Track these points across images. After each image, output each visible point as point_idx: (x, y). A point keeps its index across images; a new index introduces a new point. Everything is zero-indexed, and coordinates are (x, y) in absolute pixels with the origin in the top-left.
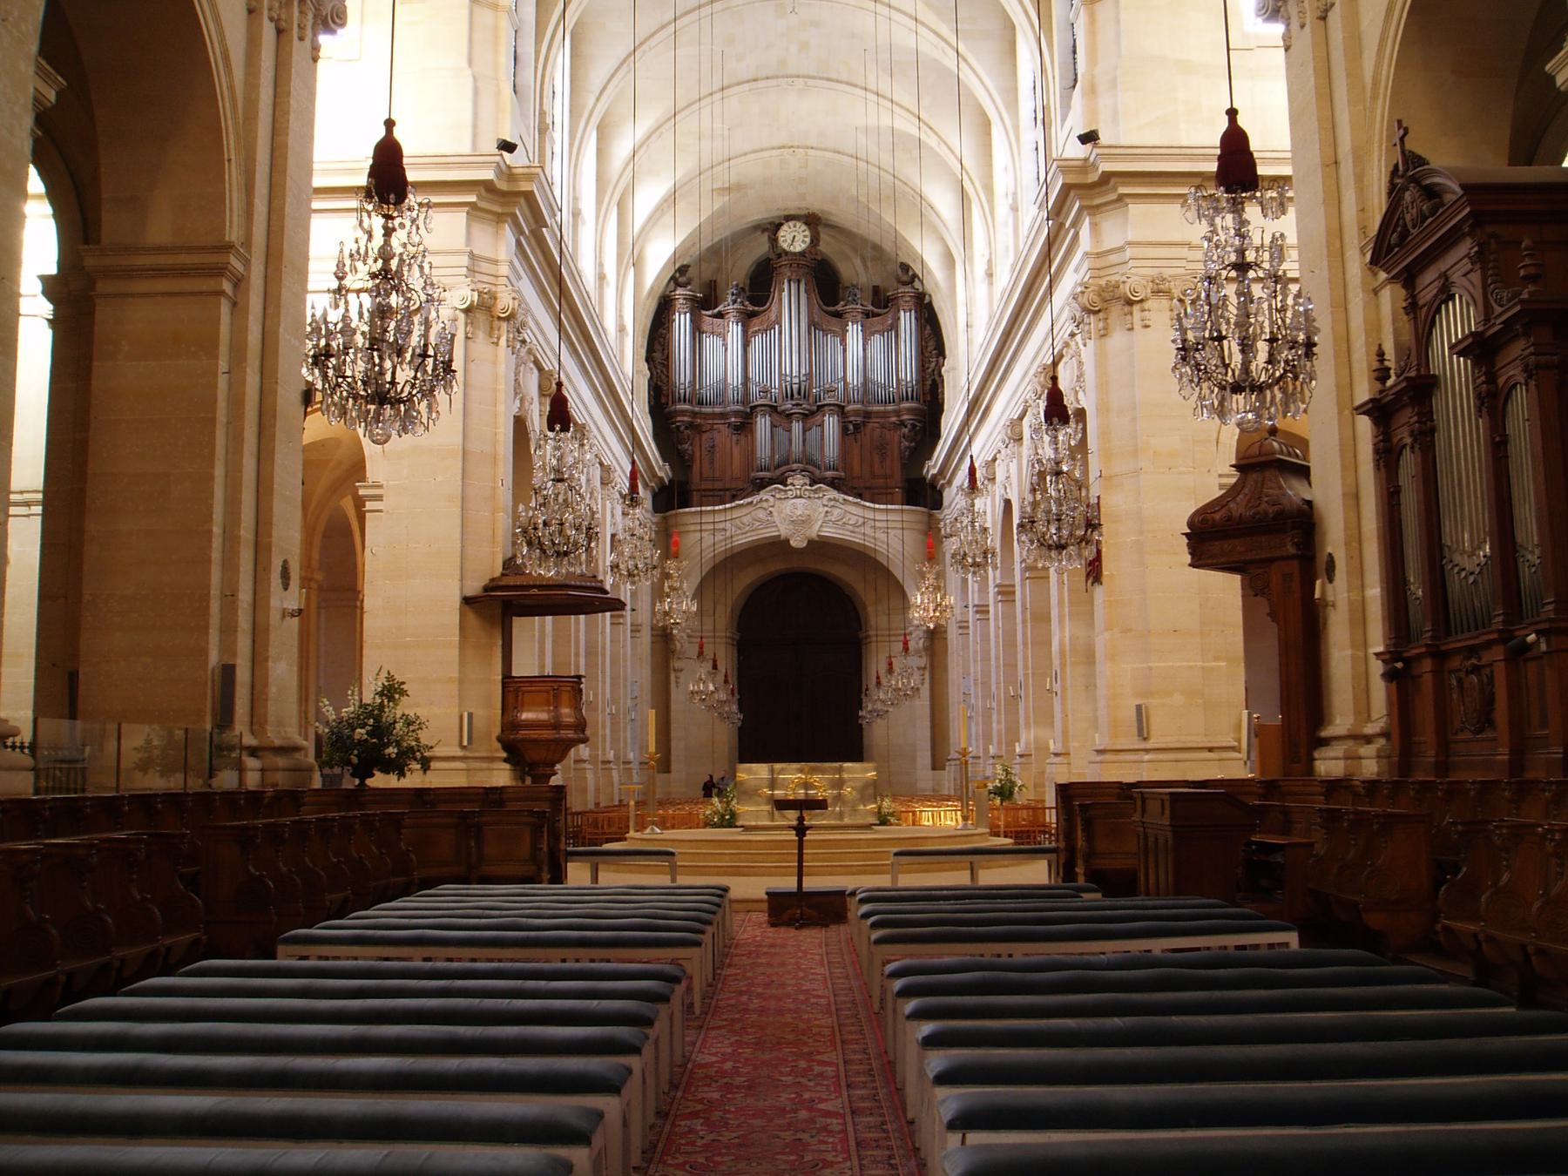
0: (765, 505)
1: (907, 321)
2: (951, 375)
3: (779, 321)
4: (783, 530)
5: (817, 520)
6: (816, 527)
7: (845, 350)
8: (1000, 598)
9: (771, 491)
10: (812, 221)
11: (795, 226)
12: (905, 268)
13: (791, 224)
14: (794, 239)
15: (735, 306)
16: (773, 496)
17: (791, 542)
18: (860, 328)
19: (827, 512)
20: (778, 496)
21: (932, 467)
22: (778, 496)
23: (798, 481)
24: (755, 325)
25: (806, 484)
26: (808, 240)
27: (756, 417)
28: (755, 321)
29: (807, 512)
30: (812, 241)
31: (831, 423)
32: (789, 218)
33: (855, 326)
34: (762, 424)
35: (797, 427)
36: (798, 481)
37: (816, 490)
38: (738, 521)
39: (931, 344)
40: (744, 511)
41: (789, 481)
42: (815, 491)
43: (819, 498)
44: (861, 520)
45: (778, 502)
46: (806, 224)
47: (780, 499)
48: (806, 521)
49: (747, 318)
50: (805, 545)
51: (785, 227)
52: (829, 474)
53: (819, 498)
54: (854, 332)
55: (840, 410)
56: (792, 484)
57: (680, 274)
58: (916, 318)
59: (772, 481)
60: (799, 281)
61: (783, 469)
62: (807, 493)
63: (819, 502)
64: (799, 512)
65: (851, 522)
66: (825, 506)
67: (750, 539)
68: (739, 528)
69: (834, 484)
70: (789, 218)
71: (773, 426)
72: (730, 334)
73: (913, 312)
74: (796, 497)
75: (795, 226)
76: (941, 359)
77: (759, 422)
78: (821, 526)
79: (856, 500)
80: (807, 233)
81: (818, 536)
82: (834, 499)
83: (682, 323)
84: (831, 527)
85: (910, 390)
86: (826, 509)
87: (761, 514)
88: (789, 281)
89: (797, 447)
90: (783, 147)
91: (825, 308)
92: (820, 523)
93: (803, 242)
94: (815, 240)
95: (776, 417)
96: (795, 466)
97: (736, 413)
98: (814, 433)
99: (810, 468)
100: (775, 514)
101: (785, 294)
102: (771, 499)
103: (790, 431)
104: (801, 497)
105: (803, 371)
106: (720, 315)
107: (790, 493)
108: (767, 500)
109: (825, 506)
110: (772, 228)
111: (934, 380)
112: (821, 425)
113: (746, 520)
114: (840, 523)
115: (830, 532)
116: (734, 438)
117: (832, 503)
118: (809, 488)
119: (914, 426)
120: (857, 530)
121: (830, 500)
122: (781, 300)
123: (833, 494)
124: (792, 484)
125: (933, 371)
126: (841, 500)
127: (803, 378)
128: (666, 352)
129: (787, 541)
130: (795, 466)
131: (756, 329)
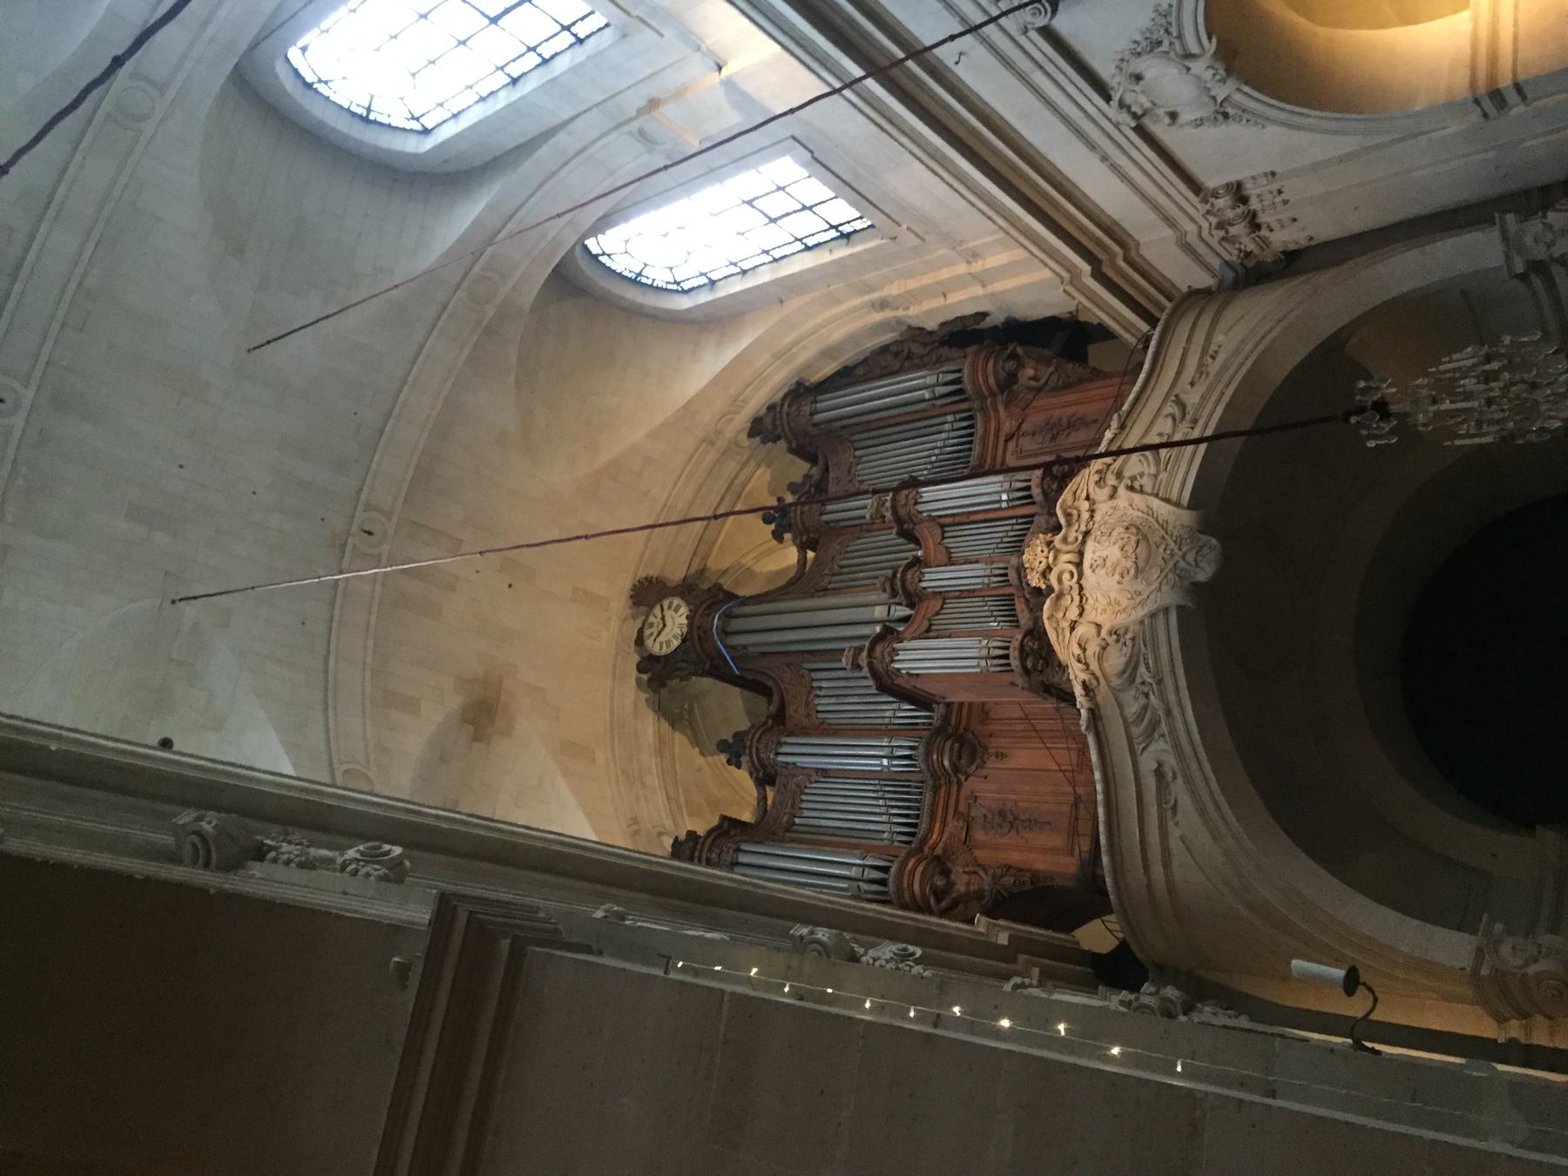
5: (1150, 511)
6: (1162, 509)
12: (757, 428)
16: (1072, 629)
17: (1202, 577)
19: (1131, 488)
20: (1073, 613)
28: (790, 710)
32: (640, 641)
37: (1068, 516)
38: (1137, 731)
41: (1035, 580)
43: (1092, 511)
44: (1171, 408)
45: (1090, 614)
50: (1214, 541)
53: (1092, 511)
63: (1103, 509)
64: (1114, 553)
66: (1113, 495)
67: (1185, 693)
68: (1154, 725)
74: (1079, 565)
78: (1167, 500)
79: (1114, 424)
81: (1193, 505)
84: (1172, 475)
86: (1122, 490)
90: (344, 545)
102: (1080, 631)
104: (1081, 554)
107: (1066, 576)
111: (943, 343)
116: (992, 763)
119: (1013, 356)
129: (1196, 589)
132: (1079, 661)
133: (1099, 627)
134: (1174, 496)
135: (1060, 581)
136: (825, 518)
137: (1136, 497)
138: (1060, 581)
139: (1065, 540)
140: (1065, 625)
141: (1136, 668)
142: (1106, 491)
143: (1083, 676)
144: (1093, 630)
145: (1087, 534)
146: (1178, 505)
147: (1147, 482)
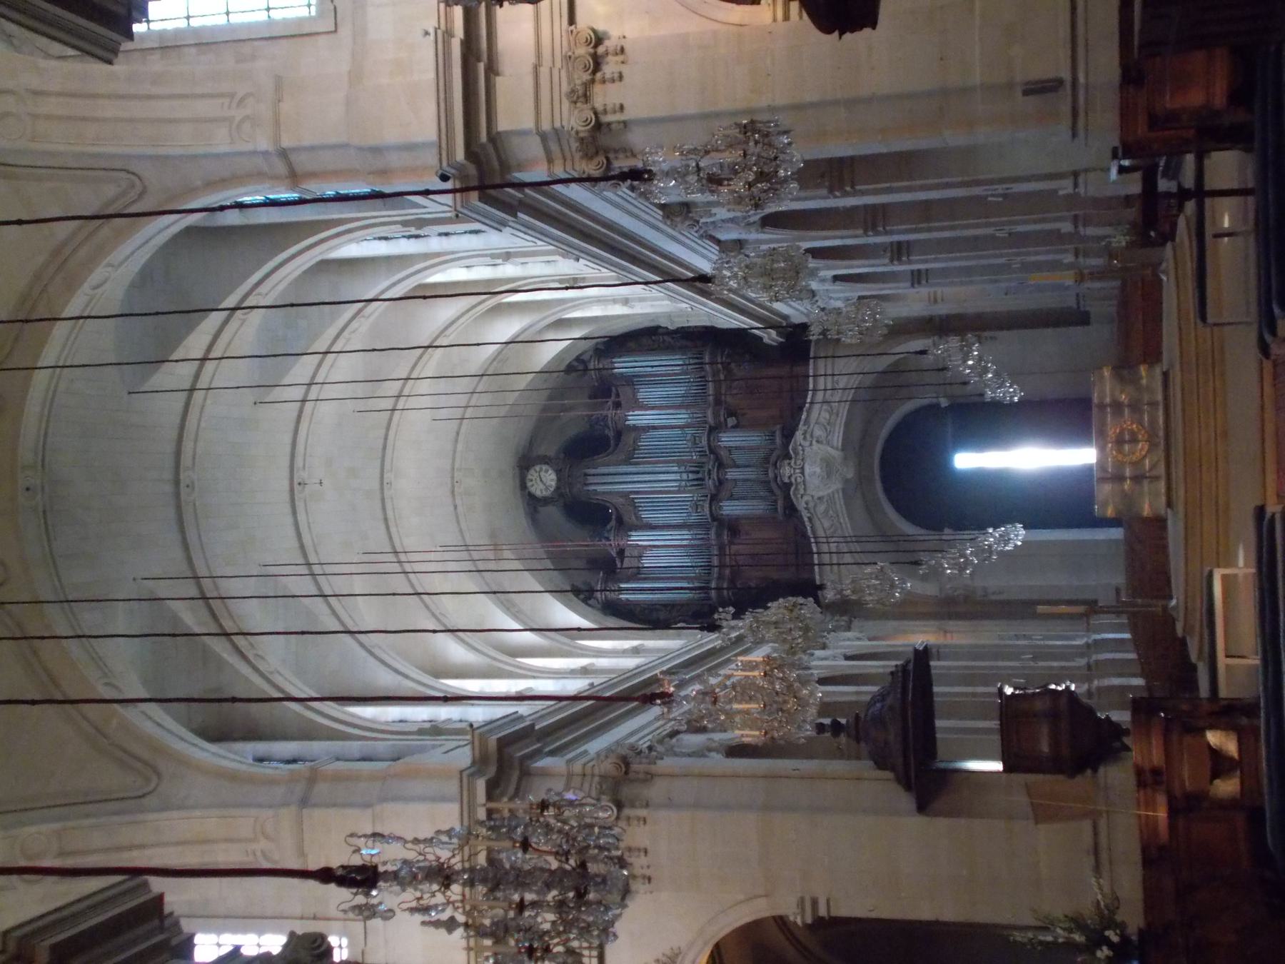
0: (811, 505)
1: (624, 365)
2: (676, 320)
3: (625, 495)
4: (836, 485)
7: (655, 428)
8: (904, 258)
9: (797, 498)
10: (525, 463)
11: (532, 480)
12: (570, 369)
13: (529, 484)
14: (544, 480)
15: (612, 538)
18: (631, 413)
19: (818, 442)
21: (771, 337)
22: (802, 492)
23: (786, 471)
24: (630, 518)
25: (789, 464)
26: (544, 467)
27: (722, 515)
28: (626, 518)
29: (818, 460)
30: (546, 463)
31: (728, 439)
32: (523, 486)
33: (630, 418)
34: (730, 508)
35: (732, 474)
36: (786, 471)
37: (795, 453)
39: (645, 341)
40: (817, 524)
41: (786, 480)
42: (796, 453)
45: (808, 492)
46: (528, 469)
47: (805, 489)
48: (828, 465)
49: (624, 526)
51: (533, 490)
52: (778, 440)
53: (803, 450)
54: (637, 418)
55: (714, 430)
56: (789, 477)
57: (581, 595)
58: (620, 357)
59: (787, 498)
60: (586, 475)
61: (773, 485)
62: (798, 462)
63: (807, 449)
64: (818, 470)
65: (828, 417)
69: (788, 435)
70: (523, 486)
71: (731, 498)
72: (640, 543)
73: (614, 360)
74: (803, 473)
75: (532, 480)
76: (660, 331)
77: (728, 512)
80: (537, 468)
82: (804, 434)
83: (631, 593)
85: (692, 361)
86: (814, 442)
87: (821, 508)
88: (586, 485)
89: (751, 474)
91: (611, 449)
92: (829, 449)
93: (547, 471)
94: (545, 460)
95: (723, 494)
96: (771, 475)
97: (719, 535)
98: (739, 458)
99: (773, 459)
100: (821, 494)
101: (600, 488)
102: (806, 498)
103: (735, 480)
104: (803, 468)
105: (676, 469)
106: (621, 553)
107: (798, 478)
108: (807, 503)
109: (811, 444)
110: (533, 503)
112: (729, 449)
113: (827, 524)
114: (828, 427)
115: (837, 439)
117: (808, 436)
118: (793, 461)
120: (835, 411)
121: (805, 439)
122: (604, 493)
123: (799, 435)
124: (789, 477)
125: (673, 338)
126: (805, 428)
127: (683, 469)
128: (657, 606)
130: (771, 475)
131: (633, 518)
132: (806, 508)
133: (812, 496)
134: (835, 444)
135: (796, 480)
136: (627, 423)
137: (820, 446)
138: (796, 480)
139: (795, 463)
140: (799, 496)
141: (828, 511)
142: (807, 444)
143: (809, 515)
144: (810, 498)
145: (803, 460)
146: (837, 449)
147: (823, 438)
